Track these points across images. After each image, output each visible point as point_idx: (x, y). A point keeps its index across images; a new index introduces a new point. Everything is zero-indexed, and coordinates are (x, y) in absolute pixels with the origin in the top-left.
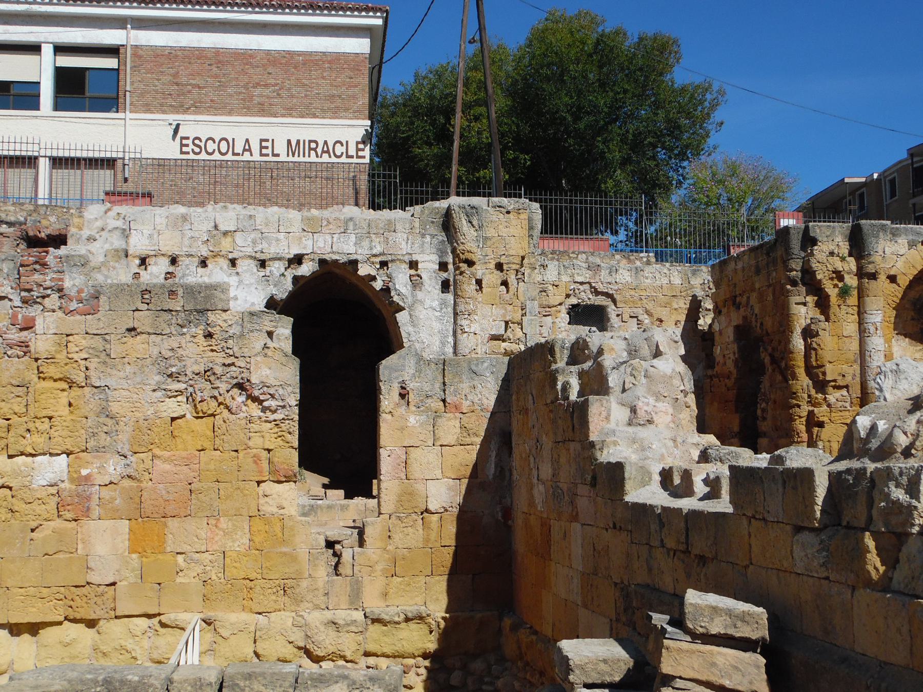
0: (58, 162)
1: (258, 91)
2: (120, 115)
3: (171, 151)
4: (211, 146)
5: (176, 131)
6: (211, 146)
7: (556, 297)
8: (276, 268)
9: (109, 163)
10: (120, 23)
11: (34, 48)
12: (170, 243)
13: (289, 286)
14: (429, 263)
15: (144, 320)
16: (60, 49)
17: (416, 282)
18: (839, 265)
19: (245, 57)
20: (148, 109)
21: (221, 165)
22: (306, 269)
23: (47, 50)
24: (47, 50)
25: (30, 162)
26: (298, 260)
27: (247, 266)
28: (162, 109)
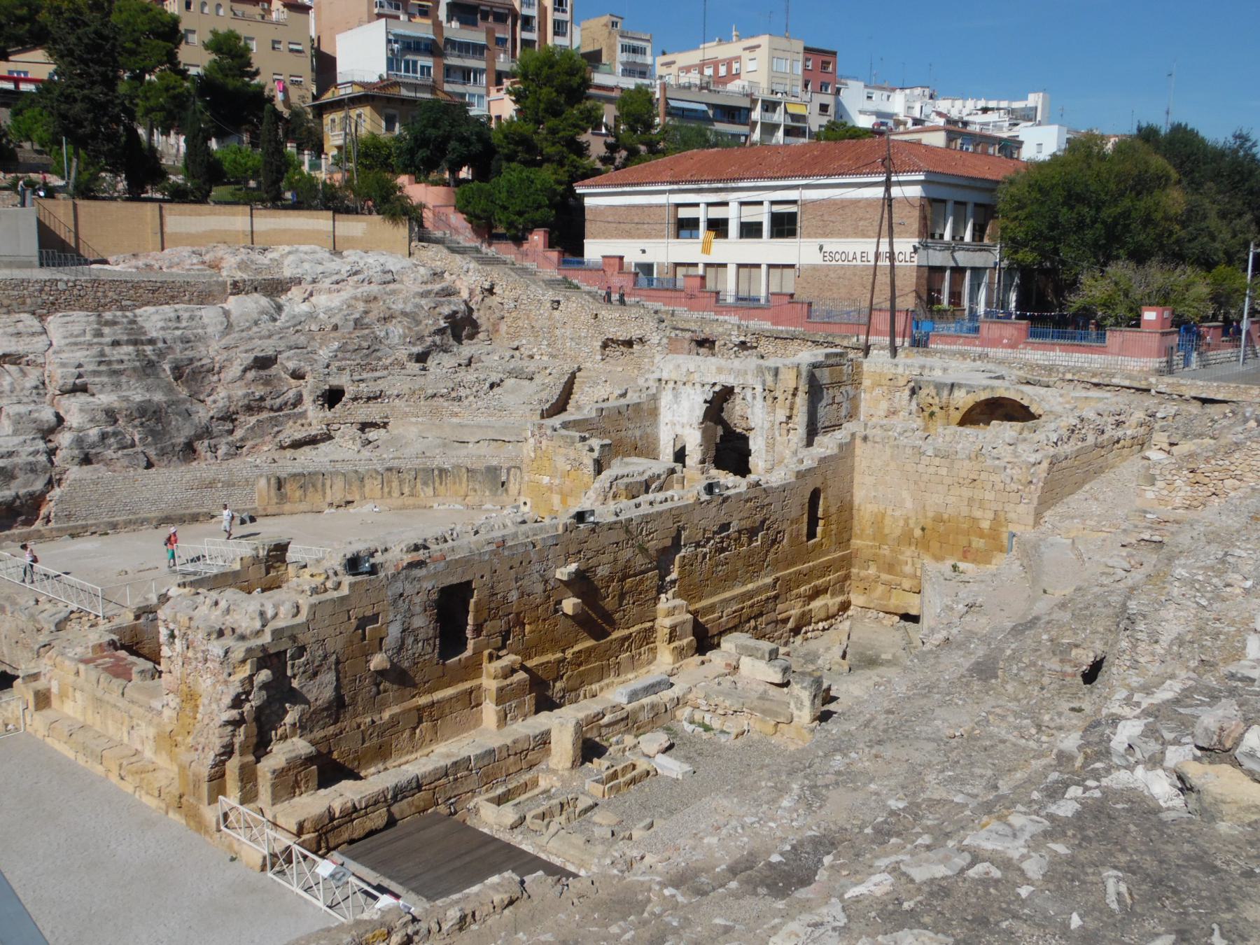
0: (770, 266)
1: (861, 223)
2: (797, 240)
3: (817, 259)
4: (838, 257)
5: (821, 248)
6: (838, 257)
7: (902, 382)
8: (707, 387)
9: (792, 266)
10: (796, 187)
11: (761, 203)
12: (674, 376)
13: (711, 395)
14: (759, 389)
15: (562, 443)
16: (773, 203)
17: (754, 398)
18: (931, 401)
19: (855, 202)
20: (809, 236)
21: (842, 267)
22: (717, 388)
23: (766, 204)
24: (766, 204)
25: (758, 266)
26: (714, 384)
27: (698, 386)
28: (816, 235)
